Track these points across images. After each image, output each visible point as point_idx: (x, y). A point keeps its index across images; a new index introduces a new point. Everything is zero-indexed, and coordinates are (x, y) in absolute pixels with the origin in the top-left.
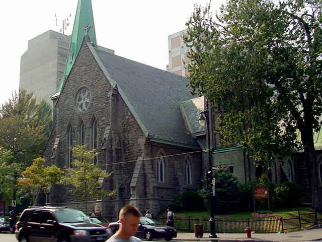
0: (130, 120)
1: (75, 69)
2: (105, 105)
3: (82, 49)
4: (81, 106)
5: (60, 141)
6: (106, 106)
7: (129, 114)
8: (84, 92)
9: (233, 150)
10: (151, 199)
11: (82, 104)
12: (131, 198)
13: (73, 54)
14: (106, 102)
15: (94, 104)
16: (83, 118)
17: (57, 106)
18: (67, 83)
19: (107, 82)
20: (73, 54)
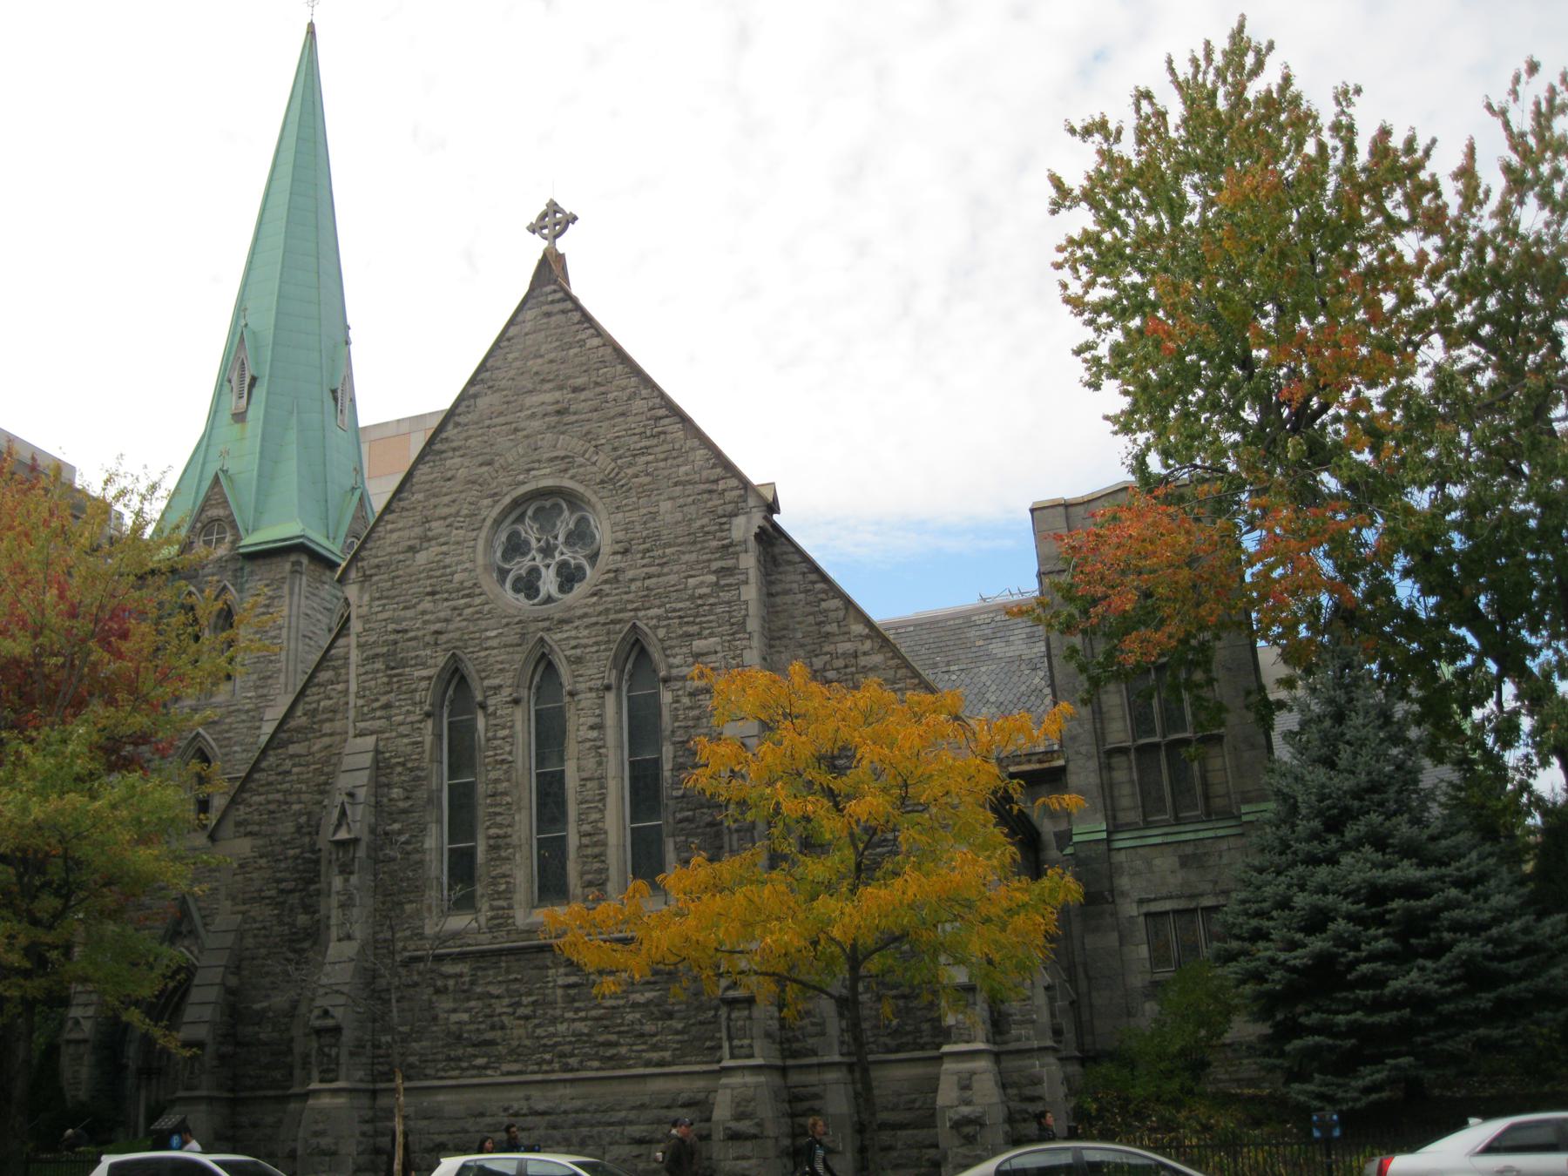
0: (863, 661)
1: (482, 403)
2: (713, 578)
3: (529, 314)
4: (528, 585)
5: (377, 751)
6: (717, 584)
7: (858, 629)
8: (546, 517)
9: (1221, 833)
10: (1041, 1049)
11: (534, 572)
12: (946, 1048)
13: (254, 380)
14: (715, 565)
15: (630, 574)
16: (552, 638)
17: (353, 575)
18: (424, 469)
19: (719, 471)
20: (254, 380)
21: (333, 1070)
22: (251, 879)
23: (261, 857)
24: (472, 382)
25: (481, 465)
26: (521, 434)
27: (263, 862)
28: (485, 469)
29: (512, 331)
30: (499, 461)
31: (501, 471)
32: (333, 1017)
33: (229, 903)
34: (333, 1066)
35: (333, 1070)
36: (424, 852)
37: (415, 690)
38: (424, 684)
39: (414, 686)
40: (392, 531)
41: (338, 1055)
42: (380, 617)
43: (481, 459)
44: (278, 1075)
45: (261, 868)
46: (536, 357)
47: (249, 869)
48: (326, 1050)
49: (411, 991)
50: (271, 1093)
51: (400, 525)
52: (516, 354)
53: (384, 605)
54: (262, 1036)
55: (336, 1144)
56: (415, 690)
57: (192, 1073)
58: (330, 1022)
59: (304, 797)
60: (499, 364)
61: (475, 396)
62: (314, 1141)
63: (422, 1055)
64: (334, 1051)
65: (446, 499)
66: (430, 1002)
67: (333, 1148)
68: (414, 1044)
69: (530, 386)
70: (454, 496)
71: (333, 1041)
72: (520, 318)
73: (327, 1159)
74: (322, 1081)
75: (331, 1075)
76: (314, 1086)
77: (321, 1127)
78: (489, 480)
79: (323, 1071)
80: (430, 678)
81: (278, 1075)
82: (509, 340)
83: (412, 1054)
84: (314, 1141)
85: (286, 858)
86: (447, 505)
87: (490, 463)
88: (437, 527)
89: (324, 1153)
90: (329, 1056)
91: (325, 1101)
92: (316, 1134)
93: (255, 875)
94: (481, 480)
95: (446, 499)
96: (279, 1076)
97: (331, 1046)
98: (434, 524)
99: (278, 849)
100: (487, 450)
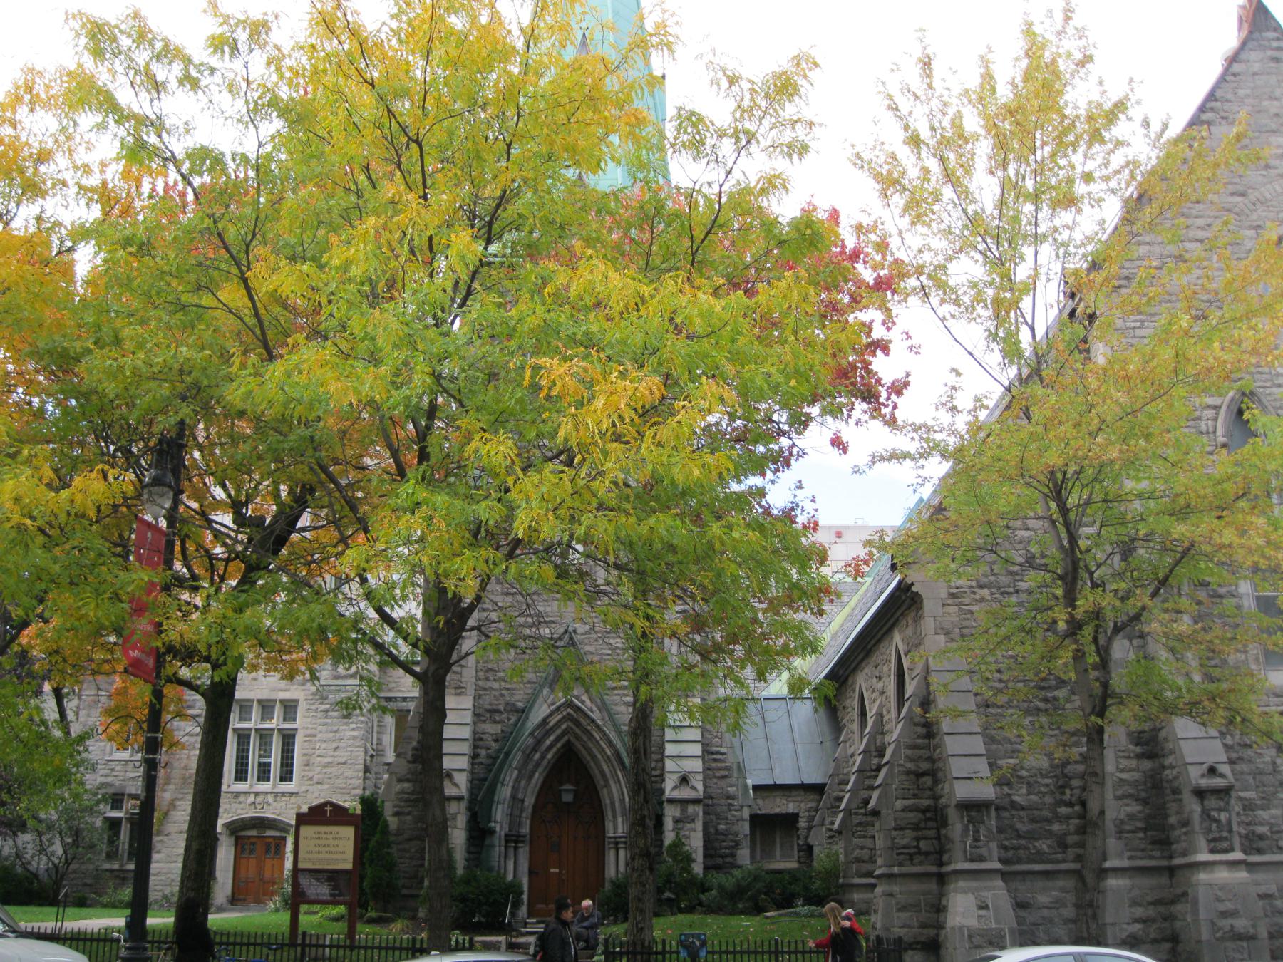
21: (1226, 839)
22: (971, 612)
23: (981, 587)
24: (1202, 109)
25: (1232, 194)
26: (1273, 172)
27: (985, 592)
28: (1239, 199)
29: (1236, 67)
30: (1253, 195)
31: (1258, 205)
32: (1222, 776)
33: (942, 638)
34: (1225, 834)
35: (1226, 839)
36: (1240, 597)
37: (1199, 418)
38: (1210, 413)
39: (1197, 414)
40: (1139, 244)
41: (1229, 822)
42: (1139, 332)
43: (1231, 188)
44: (1044, 845)
45: (983, 600)
46: (1271, 98)
47: (967, 601)
48: (1214, 814)
49: (1249, 752)
50: (1037, 867)
51: (1147, 239)
52: (1248, 92)
53: (1142, 321)
54: (1016, 798)
55: (1254, 926)
56: (1199, 418)
57: (976, 840)
58: (1217, 782)
59: (1031, 523)
60: (1230, 96)
61: (1209, 123)
62: (1225, 923)
63: (1272, 825)
64: (1223, 817)
65: (1200, 222)
66: (1274, 763)
67: (1252, 931)
68: (1260, 812)
69: (1274, 126)
70: (1209, 221)
71: (1222, 804)
72: (1243, 56)
73: (1245, 944)
74: (1212, 851)
75: (1225, 845)
76: (1204, 857)
77: (1229, 906)
78: (1246, 211)
79: (1209, 841)
80: (1217, 408)
81: (1044, 845)
82: (1234, 75)
83: (1261, 824)
84: (1225, 923)
85: (1017, 592)
86: (1201, 228)
87: (1243, 195)
88: (1195, 250)
89: (1238, 937)
90: (1217, 821)
91: (1223, 875)
92: (1224, 914)
93: (975, 608)
94: (1237, 210)
95: (1200, 222)
96: (1044, 847)
97: (1220, 810)
98: (1189, 245)
99: (1004, 580)
100: (1237, 180)
